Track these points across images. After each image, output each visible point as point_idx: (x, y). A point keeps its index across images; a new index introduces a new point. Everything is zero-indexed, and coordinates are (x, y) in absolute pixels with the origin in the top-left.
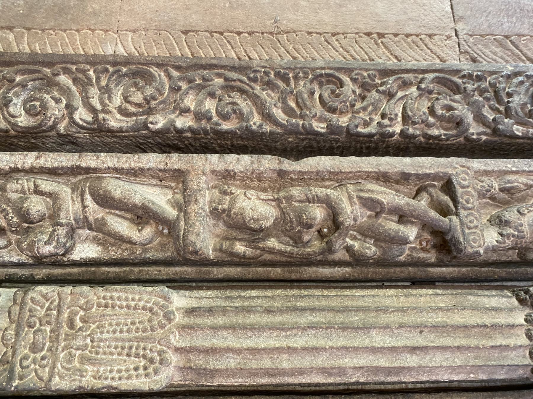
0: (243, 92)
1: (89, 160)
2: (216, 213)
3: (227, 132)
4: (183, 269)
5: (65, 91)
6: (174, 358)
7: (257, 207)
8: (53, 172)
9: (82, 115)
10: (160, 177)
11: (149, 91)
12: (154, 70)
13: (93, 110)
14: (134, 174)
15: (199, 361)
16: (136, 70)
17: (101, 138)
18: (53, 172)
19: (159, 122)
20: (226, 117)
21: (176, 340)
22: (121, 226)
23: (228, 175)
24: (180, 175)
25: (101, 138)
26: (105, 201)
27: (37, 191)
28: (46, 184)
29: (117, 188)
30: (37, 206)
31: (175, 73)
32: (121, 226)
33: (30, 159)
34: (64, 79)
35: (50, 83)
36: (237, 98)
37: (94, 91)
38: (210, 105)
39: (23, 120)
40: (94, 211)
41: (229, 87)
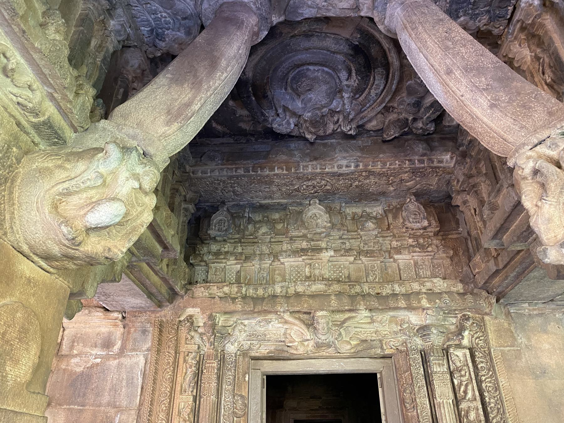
0: (498, 412)
1: (474, 381)
2: (469, 407)
3: (487, 410)
4: (457, 402)
5: (488, 373)
6: (441, 401)
7: (472, 416)
8: (470, 374)
9: (483, 378)
10: (474, 395)
11: (492, 391)
12: (498, 392)
13: (485, 380)
14: (473, 390)
15: (442, 405)
16: (497, 389)
17: (479, 383)
18: (470, 374)
19: (486, 394)
20: (491, 408)
21: (444, 401)
22: (462, 388)
23: (478, 409)
24: (475, 399)
25: (479, 383)
26: (467, 386)
27: (466, 372)
28: (467, 374)
29: (470, 387)
30: (463, 373)
31: (498, 397)
32: (462, 388)
33: (472, 370)
34: (491, 373)
35: (489, 370)
36: (496, 411)
37: (490, 380)
38: (492, 405)
39: (479, 366)
40: (464, 383)
41: (498, 409)
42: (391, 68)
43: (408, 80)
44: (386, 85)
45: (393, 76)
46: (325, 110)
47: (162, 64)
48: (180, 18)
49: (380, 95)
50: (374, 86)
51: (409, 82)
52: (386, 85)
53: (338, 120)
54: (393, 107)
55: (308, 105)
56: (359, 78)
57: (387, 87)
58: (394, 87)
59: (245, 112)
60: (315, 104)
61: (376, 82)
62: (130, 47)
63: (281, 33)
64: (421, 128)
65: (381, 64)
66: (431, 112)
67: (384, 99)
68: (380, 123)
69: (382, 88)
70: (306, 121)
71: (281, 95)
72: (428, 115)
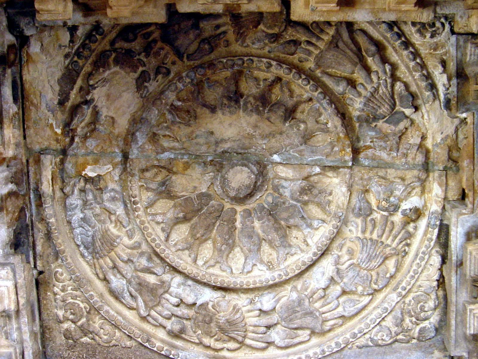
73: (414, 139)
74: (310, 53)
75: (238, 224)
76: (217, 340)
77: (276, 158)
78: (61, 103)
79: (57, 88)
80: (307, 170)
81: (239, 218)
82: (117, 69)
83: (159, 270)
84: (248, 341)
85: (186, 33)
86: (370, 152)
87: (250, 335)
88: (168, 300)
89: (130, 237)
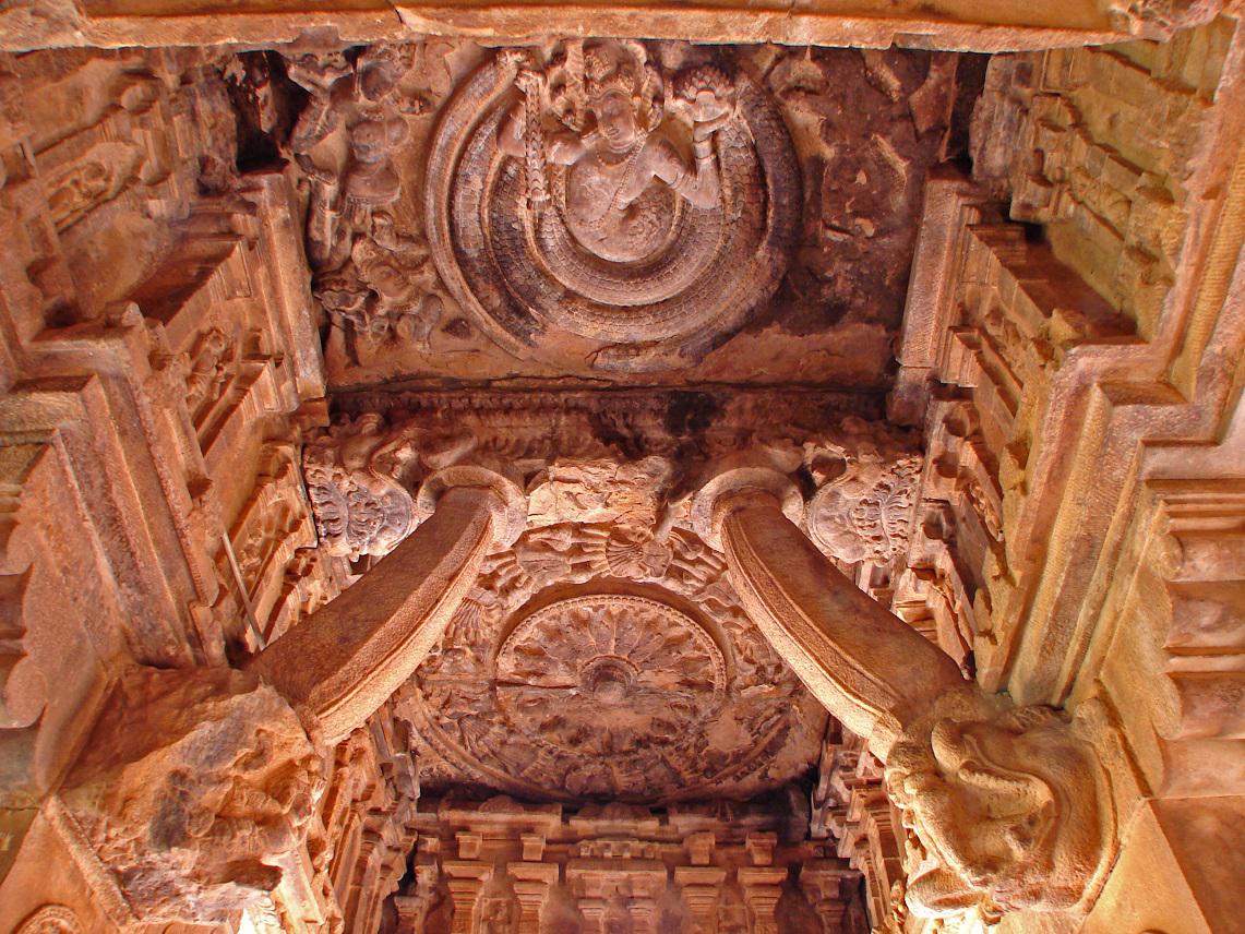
42: (449, 247)
43: (399, 201)
44: (451, 207)
45: (439, 228)
46: (588, 143)
47: (920, 380)
48: (838, 520)
49: (455, 175)
50: (476, 201)
51: (397, 197)
52: (451, 207)
53: (553, 97)
54: (414, 113)
55: (634, 177)
56: (515, 226)
57: (446, 189)
58: (431, 202)
59: (803, 115)
60: (614, 177)
61: (474, 215)
62: (937, 501)
63: (682, 355)
64: (322, 72)
65: (473, 267)
66: (318, 128)
67: (445, 159)
68: (435, 63)
69: (459, 201)
70: (642, 121)
71: (702, 193)
72: (323, 116)
73: (437, 701)
74: (544, 759)
75: (613, 643)
76: (641, 535)
77: (573, 692)
78: (787, 728)
79: (788, 741)
80: (541, 682)
81: (612, 647)
82: (726, 752)
83: (704, 608)
84: (605, 534)
85: (656, 775)
86: (479, 690)
87: (603, 542)
88: (699, 580)
89: (733, 636)
